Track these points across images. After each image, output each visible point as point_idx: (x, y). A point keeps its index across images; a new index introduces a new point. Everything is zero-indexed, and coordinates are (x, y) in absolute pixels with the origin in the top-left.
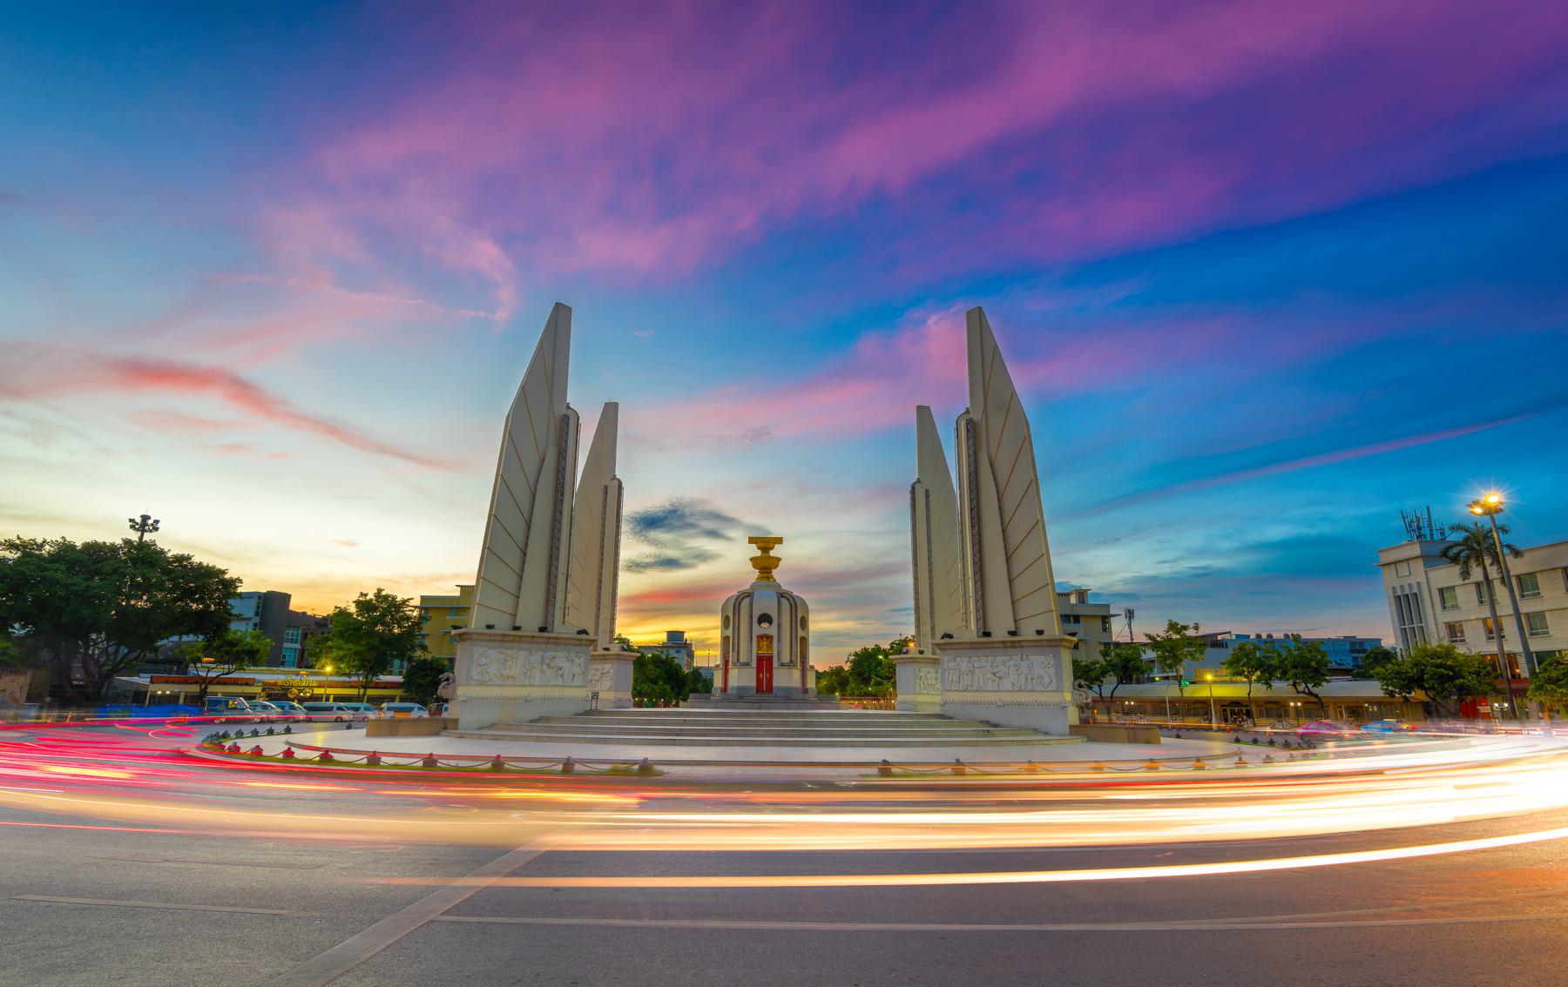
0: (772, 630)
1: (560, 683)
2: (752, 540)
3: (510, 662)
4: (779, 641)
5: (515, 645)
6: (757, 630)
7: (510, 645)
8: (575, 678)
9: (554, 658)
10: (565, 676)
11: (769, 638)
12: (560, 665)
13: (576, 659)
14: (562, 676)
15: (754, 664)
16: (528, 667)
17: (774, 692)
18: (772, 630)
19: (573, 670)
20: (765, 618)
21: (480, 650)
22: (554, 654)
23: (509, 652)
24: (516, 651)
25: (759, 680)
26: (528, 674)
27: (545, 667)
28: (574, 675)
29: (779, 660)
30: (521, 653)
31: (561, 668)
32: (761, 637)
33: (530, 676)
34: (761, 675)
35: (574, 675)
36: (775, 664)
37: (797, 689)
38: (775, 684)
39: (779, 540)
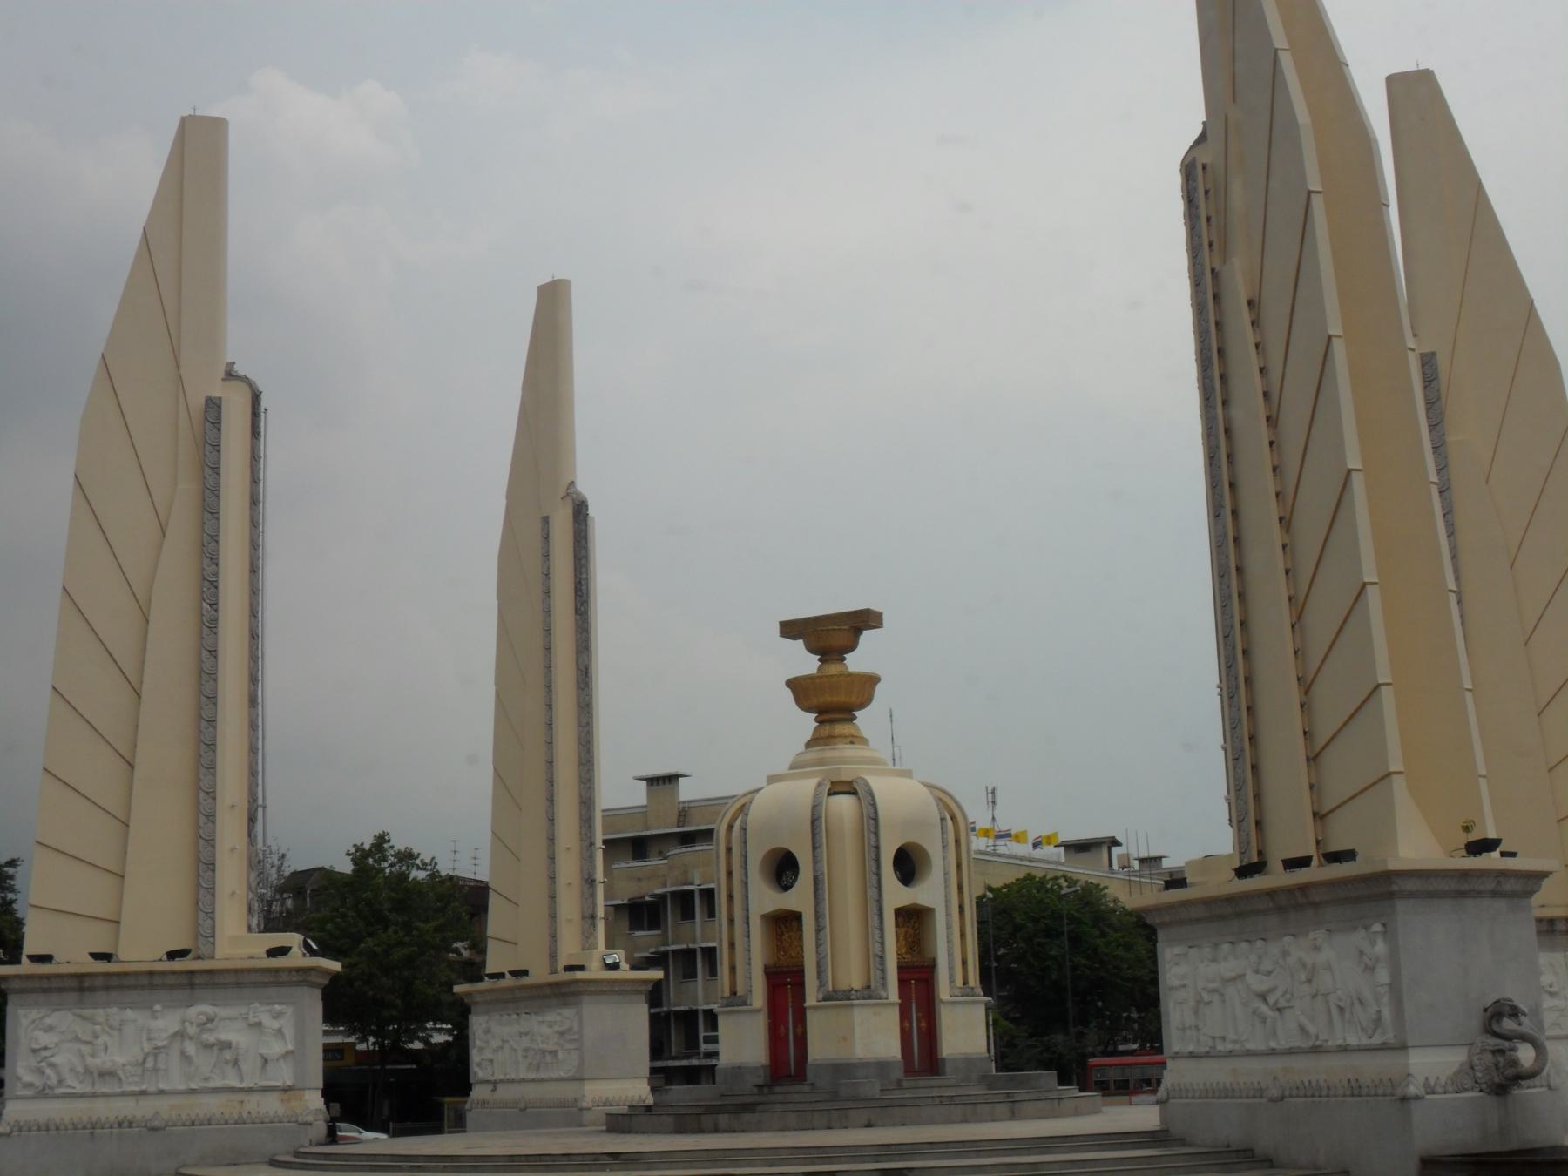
0: (798, 898)
2: (790, 629)
3: (100, 1041)
4: (819, 930)
6: (765, 899)
8: (269, 1067)
9: (211, 1020)
10: (245, 1067)
11: (796, 917)
12: (224, 1037)
13: (267, 1020)
14: (236, 1063)
15: (759, 998)
16: (147, 1047)
17: (810, 1074)
18: (798, 898)
19: (264, 1051)
20: (783, 868)
21: (34, 1014)
22: (208, 1009)
23: (100, 1014)
24: (114, 1010)
26: (150, 1064)
27: (191, 1049)
29: (822, 984)
30: (129, 1014)
31: (226, 1045)
33: (155, 1070)
34: (782, 1030)
36: (811, 999)
37: (882, 1066)
38: (810, 1059)
39: (863, 620)
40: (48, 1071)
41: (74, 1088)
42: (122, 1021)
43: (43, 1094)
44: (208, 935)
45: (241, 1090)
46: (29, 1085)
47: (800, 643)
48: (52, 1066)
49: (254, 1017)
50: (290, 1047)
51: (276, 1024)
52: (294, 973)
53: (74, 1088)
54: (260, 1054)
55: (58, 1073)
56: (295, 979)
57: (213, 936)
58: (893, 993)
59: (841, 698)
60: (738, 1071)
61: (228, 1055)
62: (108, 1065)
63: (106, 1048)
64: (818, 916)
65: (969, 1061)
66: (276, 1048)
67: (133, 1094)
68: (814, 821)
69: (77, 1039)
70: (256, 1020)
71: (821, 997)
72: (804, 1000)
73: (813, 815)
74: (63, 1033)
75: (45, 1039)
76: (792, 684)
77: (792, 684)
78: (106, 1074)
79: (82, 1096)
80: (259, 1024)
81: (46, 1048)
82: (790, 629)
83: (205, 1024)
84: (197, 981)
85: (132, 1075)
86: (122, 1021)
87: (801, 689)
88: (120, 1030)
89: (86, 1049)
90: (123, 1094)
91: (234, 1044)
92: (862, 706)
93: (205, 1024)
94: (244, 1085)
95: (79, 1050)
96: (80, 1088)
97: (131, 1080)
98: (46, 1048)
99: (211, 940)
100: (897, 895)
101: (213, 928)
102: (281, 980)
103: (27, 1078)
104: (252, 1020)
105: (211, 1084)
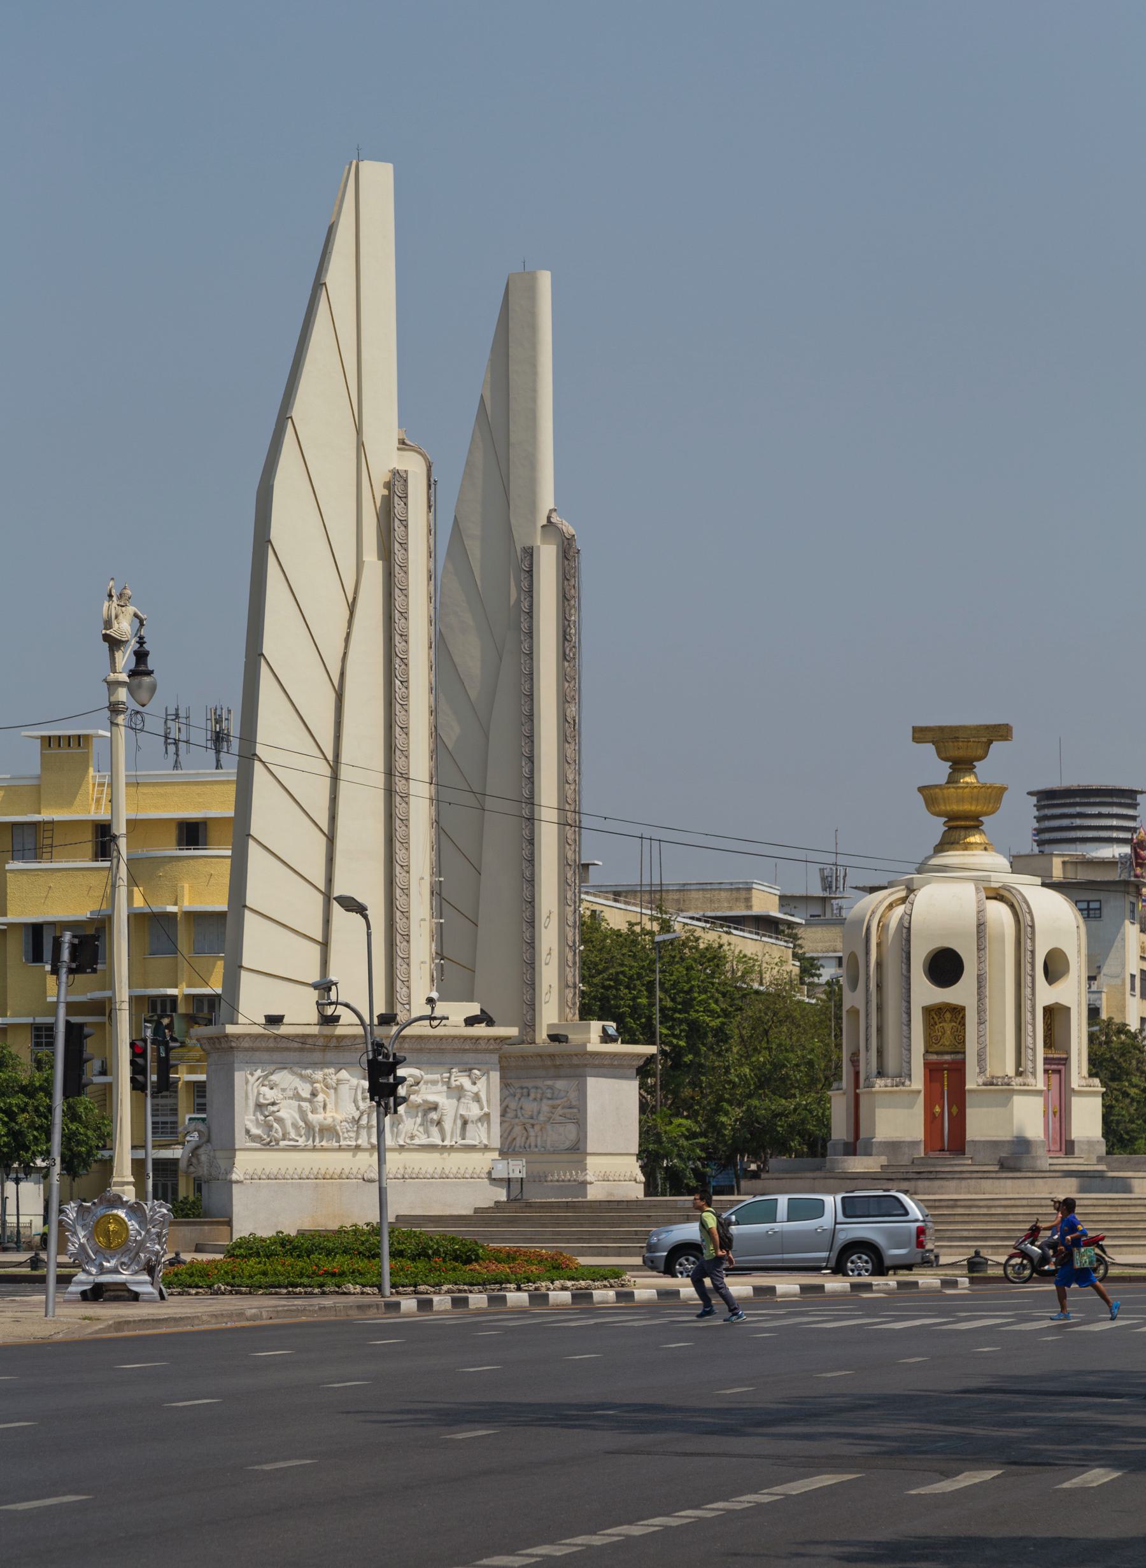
1: (440, 1143)
3: (321, 1097)
4: (981, 1022)
5: (330, 1056)
7: (317, 1056)
8: (470, 1127)
10: (448, 1125)
12: (432, 1098)
13: (465, 1082)
15: (918, 1082)
23: (319, 1075)
24: (332, 1070)
25: (932, 1121)
26: (364, 1121)
28: (465, 1123)
29: (982, 1071)
30: (344, 1074)
31: (435, 1107)
32: (934, 1013)
34: (937, 1109)
35: (465, 1123)
40: (275, 1125)
41: (297, 1141)
42: (338, 1080)
43: (269, 1145)
44: (405, 1002)
45: (444, 1147)
46: (254, 1138)
47: (930, 748)
48: (280, 1120)
49: (455, 1081)
50: (486, 1110)
51: (475, 1089)
52: (492, 1041)
53: (297, 1141)
54: (461, 1115)
55: (283, 1126)
56: (491, 1047)
57: (409, 1004)
58: (1040, 1085)
59: (967, 807)
60: (893, 1147)
61: (434, 1116)
62: (329, 1121)
63: (325, 1107)
64: (981, 1011)
65: (1090, 1143)
66: (474, 1111)
67: (348, 1149)
68: (981, 926)
69: (297, 1097)
70: (458, 1083)
71: (980, 1081)
72: (965, 1086)
73: (978, 919)
74: (284, 1090)
75: (269, 1095)
76: (921, 789)
77: (921, 789)
78: (328, 1131)
79: (304, 1149)
80: (461, 1088)
81: (273, 1104)
82: (920, 734)
83: (412, 1086)
84: (406, 1046)
85: (348, 1131)
86: (338, 1080)
87: (930, 795)
88: (335, 1089)
89: (305, 1104)
90: (340, 1149)
91: (440, 1104)
92: (986, 814)
93: (412, 1086)
94: (446, 1143)
95: (299, 1106)
96: (301, 1142)
97: (346, 1135)
98: (273, 1104)
99: (407, 1007)
100: (1046, 994)
101: (409, 996)
102: (480, 1047)
103: (255, 1131)
104: (454, 1084)
105: (417, 1141)
